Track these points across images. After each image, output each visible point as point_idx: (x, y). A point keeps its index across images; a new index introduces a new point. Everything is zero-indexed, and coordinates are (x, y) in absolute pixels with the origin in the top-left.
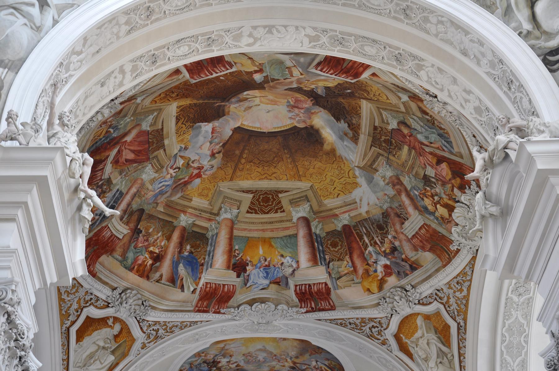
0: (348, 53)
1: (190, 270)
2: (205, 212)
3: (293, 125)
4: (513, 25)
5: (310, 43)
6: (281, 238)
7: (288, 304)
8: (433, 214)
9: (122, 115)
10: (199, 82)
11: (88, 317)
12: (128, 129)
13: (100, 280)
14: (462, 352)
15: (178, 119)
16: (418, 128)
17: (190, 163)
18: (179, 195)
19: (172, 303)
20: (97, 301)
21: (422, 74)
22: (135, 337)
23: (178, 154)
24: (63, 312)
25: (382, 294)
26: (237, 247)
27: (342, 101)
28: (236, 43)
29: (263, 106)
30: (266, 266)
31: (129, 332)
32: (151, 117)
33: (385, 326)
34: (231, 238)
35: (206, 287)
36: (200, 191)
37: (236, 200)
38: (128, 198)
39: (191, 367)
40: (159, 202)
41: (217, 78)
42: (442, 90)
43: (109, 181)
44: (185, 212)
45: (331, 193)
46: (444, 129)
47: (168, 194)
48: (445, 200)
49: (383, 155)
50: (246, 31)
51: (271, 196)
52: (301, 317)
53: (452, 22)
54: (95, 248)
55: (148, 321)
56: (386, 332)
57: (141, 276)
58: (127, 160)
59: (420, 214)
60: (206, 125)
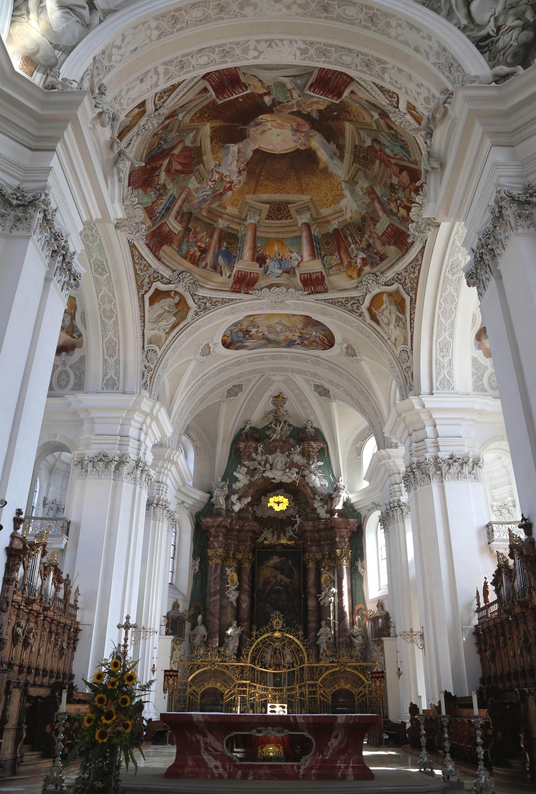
0: (330, 63)
1: (226, 261)
2: (236, 217)
3: (296, 148)
4: (454, 22)
5: (301, 55)
6: (290, 238)
7: (295, 288)
8: (396, 215)
9: (168, 129)
10: (224, 103)
11: (156, 289)
12: (175, 143)
13: (163, 263)
14: (412, 317)
15: (212, 139)
16: (386, 143)
17: (223, 177)
18: (217, 203)
19: (214, 284)
20: (162, 278)
21: (386, 76)
22: (190, 306)
23: (214, 170)
24: (139, 283)
25: (360, 279)
26: (259, 245)
27: (331, 124)
28: (245, 56)
29: (274, 130)
30: (280, 259)
31: (185, 302)
32: (191, 135)
33: (361, 302)
34: (255, 238)
35: (238, 274)
36: (232, 201)
37: (258, 209)
38: (179, 202)
39: (231, 334)
40: (202, 207)
41: (237, 99)
42: (400, 88)
43: (164, 186)
44: (222, 218)
45: (325, 204)
46: (404, 141)
47: (209, 202)
48: (405, 202)
49: (361, 170)
50: (252, 44)
51: (282, 207)
52: (305, 298)
53: (408, 23)
54: (159, 239)
55: (198, 296)
56: (362, 307)
57: (193, 263)
58: (176, 171)
59: (387, 216)
60: (233, 146)
